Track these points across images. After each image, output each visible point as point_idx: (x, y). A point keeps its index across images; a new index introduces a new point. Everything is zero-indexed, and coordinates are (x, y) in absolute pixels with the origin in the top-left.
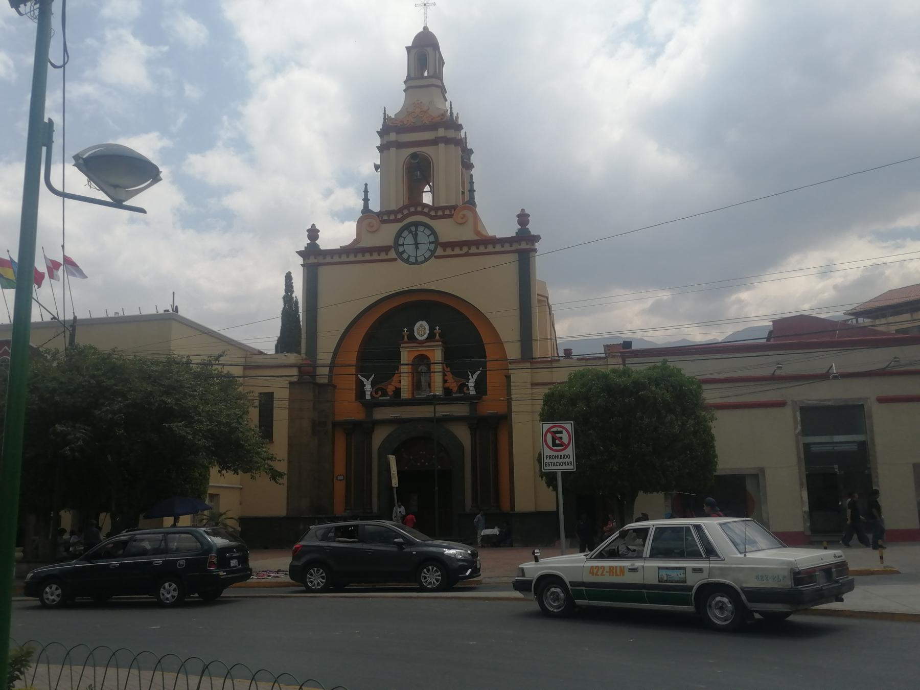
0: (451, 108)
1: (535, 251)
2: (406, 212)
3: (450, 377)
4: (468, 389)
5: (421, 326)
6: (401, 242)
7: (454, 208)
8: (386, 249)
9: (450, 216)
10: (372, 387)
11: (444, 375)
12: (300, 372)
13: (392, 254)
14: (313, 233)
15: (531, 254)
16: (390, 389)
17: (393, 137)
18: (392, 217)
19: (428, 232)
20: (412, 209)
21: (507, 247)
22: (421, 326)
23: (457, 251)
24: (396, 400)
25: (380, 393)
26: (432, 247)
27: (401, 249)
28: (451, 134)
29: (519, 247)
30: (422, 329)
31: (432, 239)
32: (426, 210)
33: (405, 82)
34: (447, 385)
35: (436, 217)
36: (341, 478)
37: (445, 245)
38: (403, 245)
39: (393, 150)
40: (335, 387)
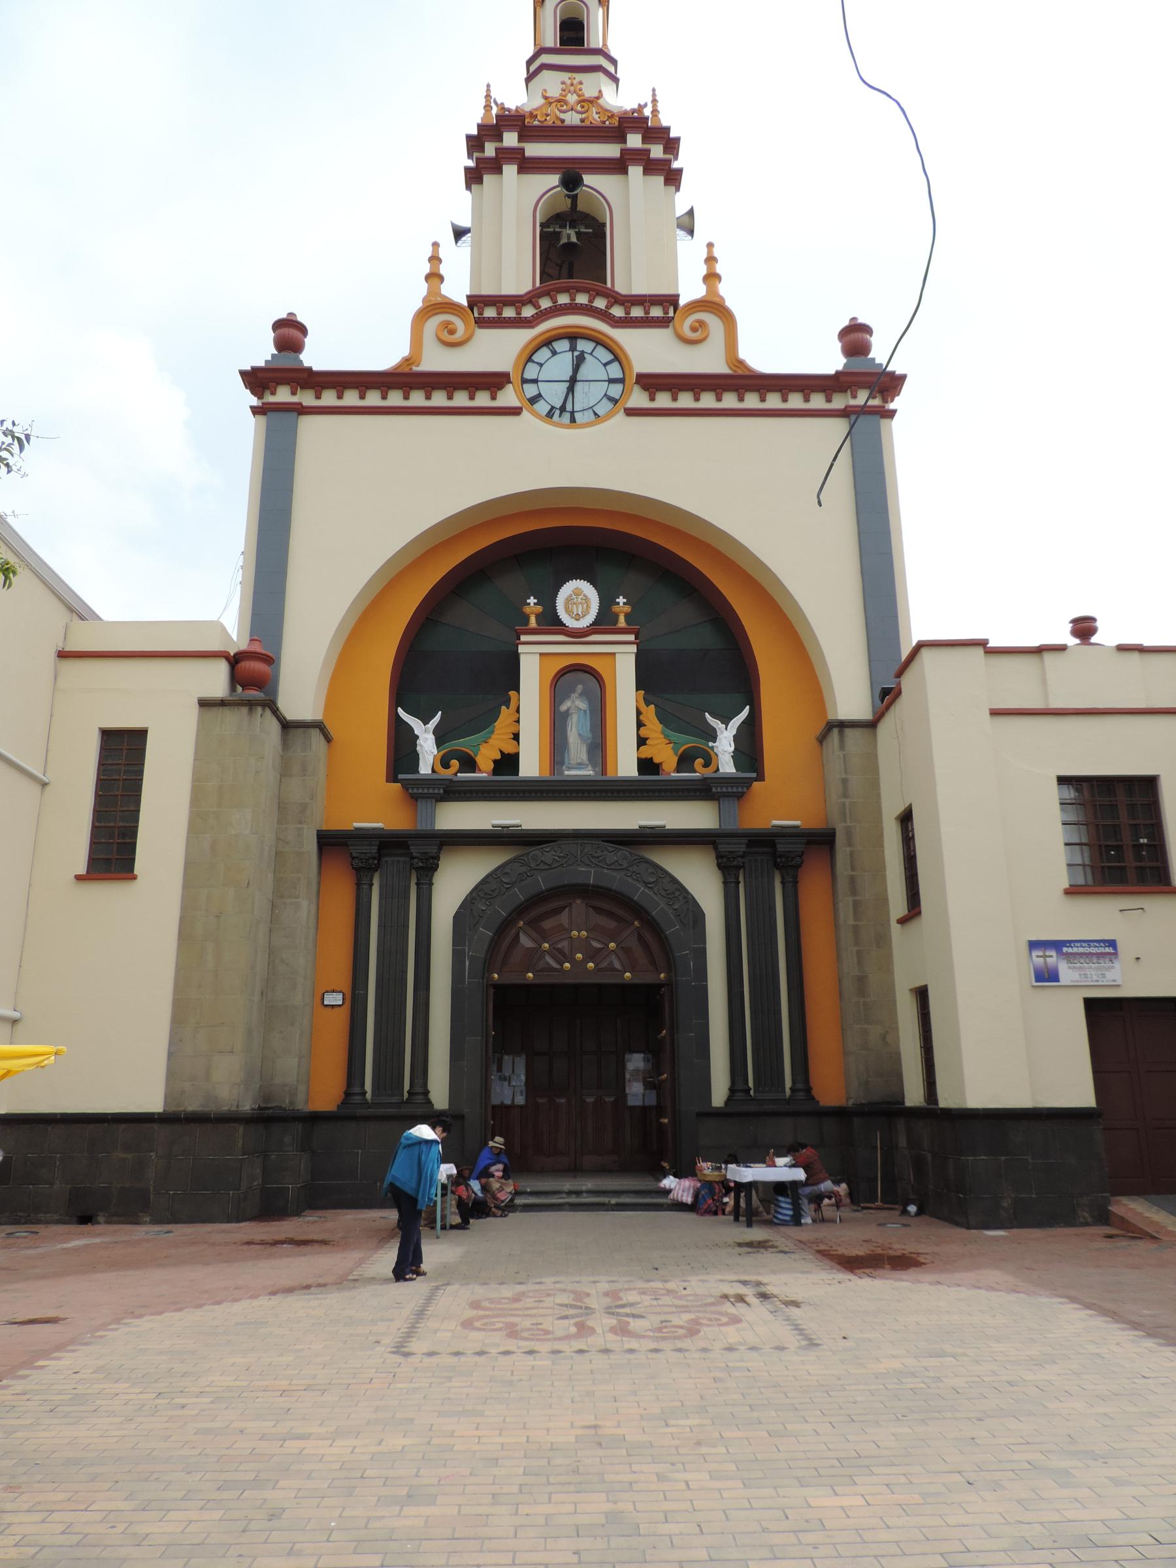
0: (654, 101)
1: (891, 414)
2: (545, 303)
3: (654, 728)
5: (578, 592)
6: (531, 372)
7: (671, 301)
8: (494, 382)
9: (663, 322)
10: (440, 742)
11: (640, 724)
12: (236, 679)
13: (508, 397)
14: (289, 333)
15: (884, 422)
16: (486, 757)
17: (510, 139)
18: (509, 312)
19: (603, 355)
20: (563, 299)
21: (818, 401)
22: (578, 592)
23: (686, 400)
25: (455, 763)
26: (615, 390)
27: (531, 391)
28: (657, 151)
29: (852, 402)
30: (578, 599)
31: (615, 371)
32: (600, 303)
33: (529, 62)
34: (646, 752)
35: (627, 322)
36: (334, 999)
37: (652, 383)
38: (535, 381)
39: (510, 170)
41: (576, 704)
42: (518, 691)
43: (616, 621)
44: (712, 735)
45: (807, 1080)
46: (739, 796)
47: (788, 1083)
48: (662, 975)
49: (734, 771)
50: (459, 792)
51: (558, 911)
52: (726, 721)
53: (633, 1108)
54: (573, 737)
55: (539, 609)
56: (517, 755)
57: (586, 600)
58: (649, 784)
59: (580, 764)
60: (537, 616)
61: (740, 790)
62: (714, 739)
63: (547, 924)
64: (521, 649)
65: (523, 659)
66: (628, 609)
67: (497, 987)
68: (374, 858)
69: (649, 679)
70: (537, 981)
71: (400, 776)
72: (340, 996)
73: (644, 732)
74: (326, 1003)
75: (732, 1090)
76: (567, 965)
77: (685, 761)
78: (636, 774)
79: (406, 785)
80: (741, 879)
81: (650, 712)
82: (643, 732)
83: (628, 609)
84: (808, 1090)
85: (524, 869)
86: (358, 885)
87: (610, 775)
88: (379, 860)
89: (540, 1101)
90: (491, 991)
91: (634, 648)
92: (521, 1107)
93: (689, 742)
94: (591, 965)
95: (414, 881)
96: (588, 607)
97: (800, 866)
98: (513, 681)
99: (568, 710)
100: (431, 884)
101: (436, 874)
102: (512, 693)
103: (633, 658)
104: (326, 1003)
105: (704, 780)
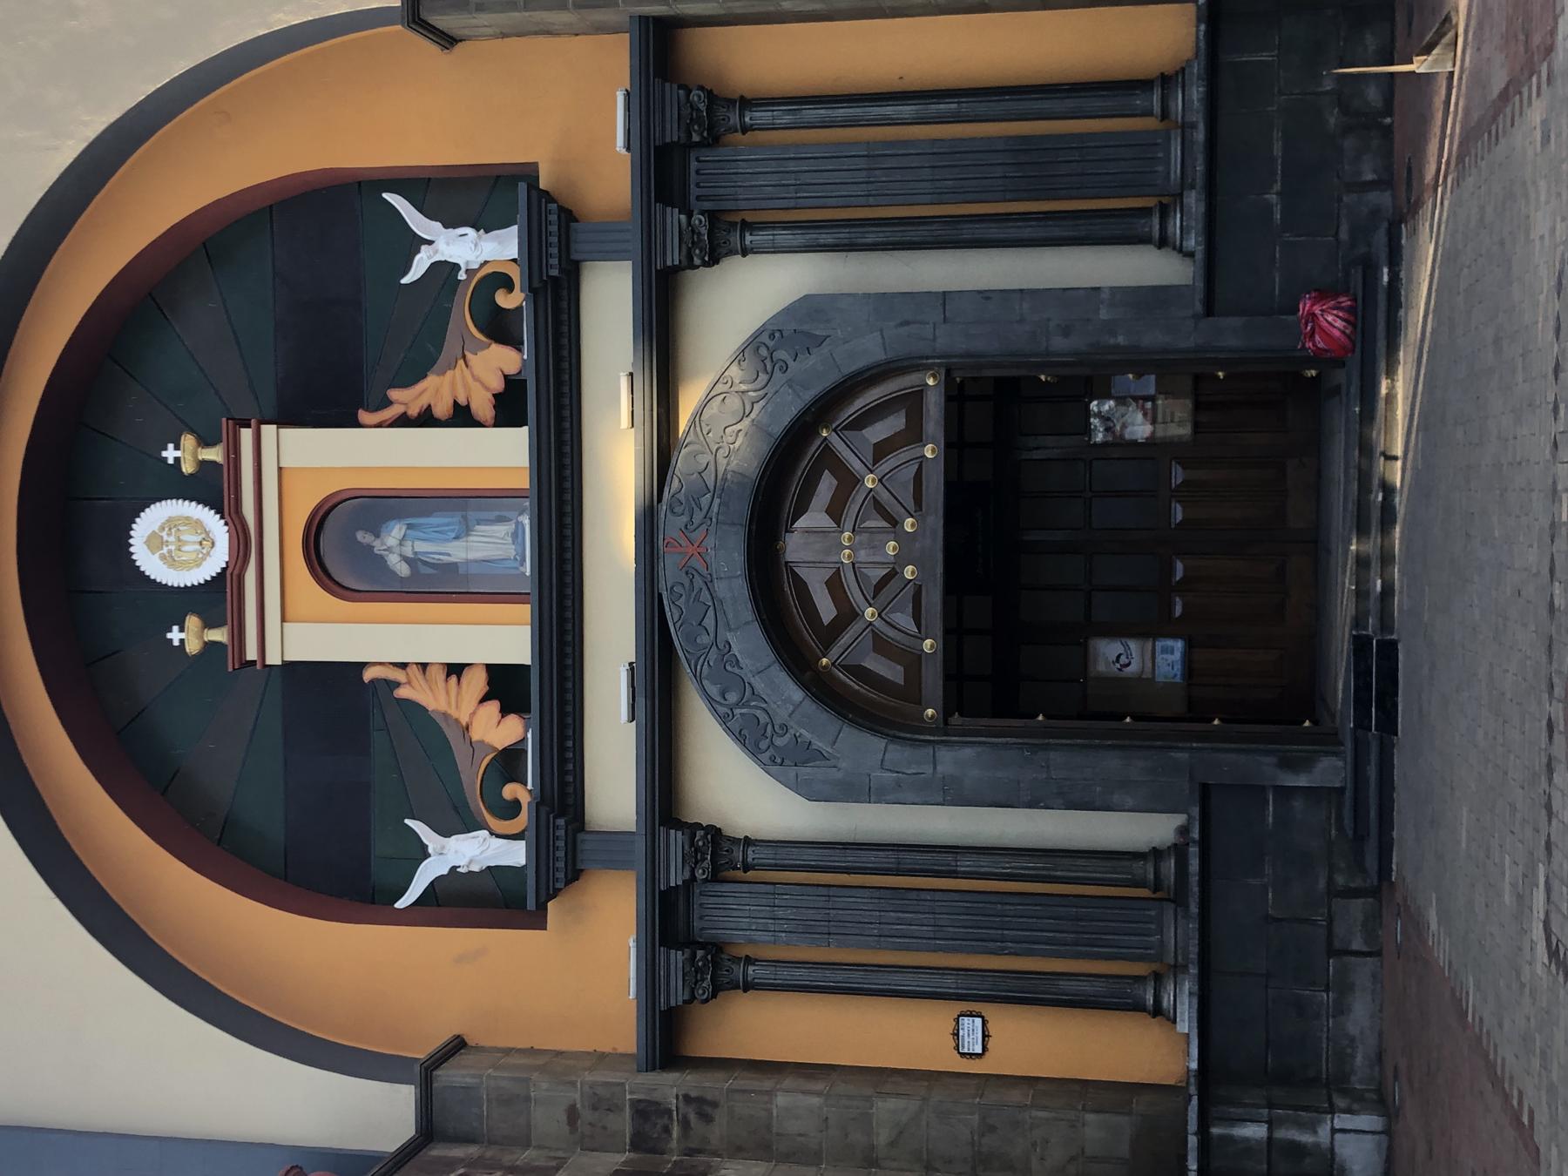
3: (435, 390)
4: (506, 282)
5: (154, 542)
11: (426, 419)
16: (499, 730)
22: (154, 542)
24: (544, 689)
25: (510, 791)
30: (173, 543)
34: (483, 406)
36: (971, 1030)
40: (457, 1045)
41: (396, 544)
42: (362, 666)
43: (214, 463)
44: (444, 272)
45: (1144, 85)
46: (568, 217)
47: (1150, 123)
48: (931, 382)
49: (515, 228)
50: (563, 784)
51: (801, 587)
52: (417, 242)
53: (1197, 427)
54: (458, 552)
55: (192, 622)
56: (490, 668)
57: (171, 524)
58: (547, 405)
59: (515, 535)
60: (209, 624)
61: (554, 218)
62: (456, 267)
63: (827, 610)
64: (273, 658)
65: (293, 655)
66: (188, 441)
67: (947, 713)
68: (694, 955)
69: (331, 400)
70: (938, 627)
71: (531, 904)
72: (966, 1021)
73: (442, 410)
74: (978, 1050)
75: (1163, 242)
76: (909, 572)
77: (499, 328)
78: (526, 428)
79: (548, 892)
80: (737, 218)
81: (406, 399)
82: (442, 410)
83: (188, 441)
84: (1167, 81)
85: (713, 655)
86: (748, 986)
87: (523, 481)
88: (703, 946)
89: (1178, 610)
90: (956, 719)
91: (269, 431)
92: (1190, 647)
93: (463, 318)
94: (909, 525)
95: (740, 874)
96: (187, 520)
97: (712, 97)
98: (341, 678)
99: (405, 559)
100: (748, 842)
101: (728, 832)
102: (368, 675)
103: (288, 433)
104: (978, 1050)
105: (533, 291)
